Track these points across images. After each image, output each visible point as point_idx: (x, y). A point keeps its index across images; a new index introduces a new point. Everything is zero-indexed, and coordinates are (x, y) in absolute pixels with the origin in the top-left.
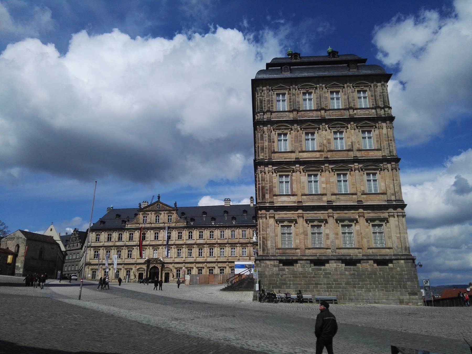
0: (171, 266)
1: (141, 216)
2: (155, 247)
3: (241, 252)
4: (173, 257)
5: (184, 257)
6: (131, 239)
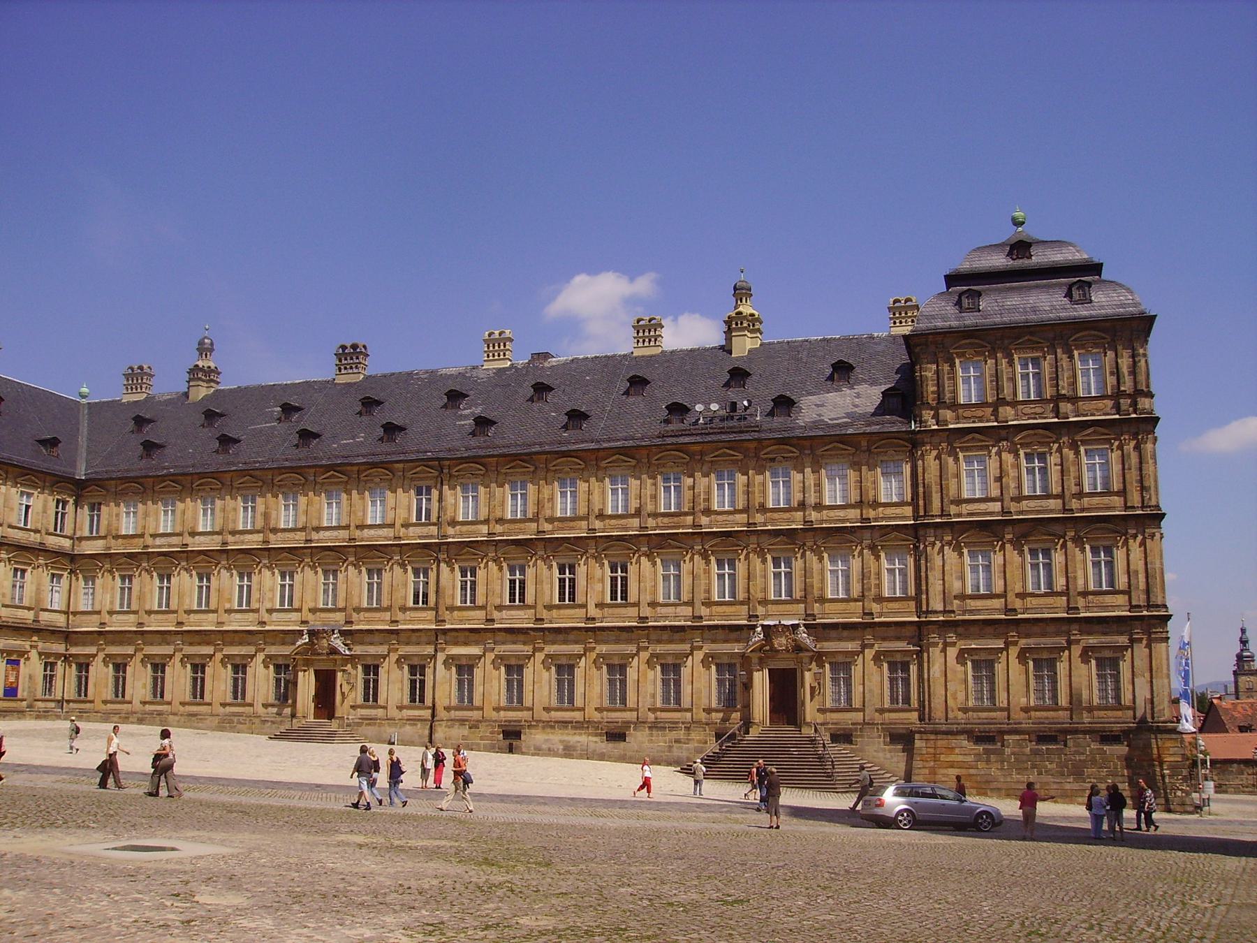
3: (8, 584)
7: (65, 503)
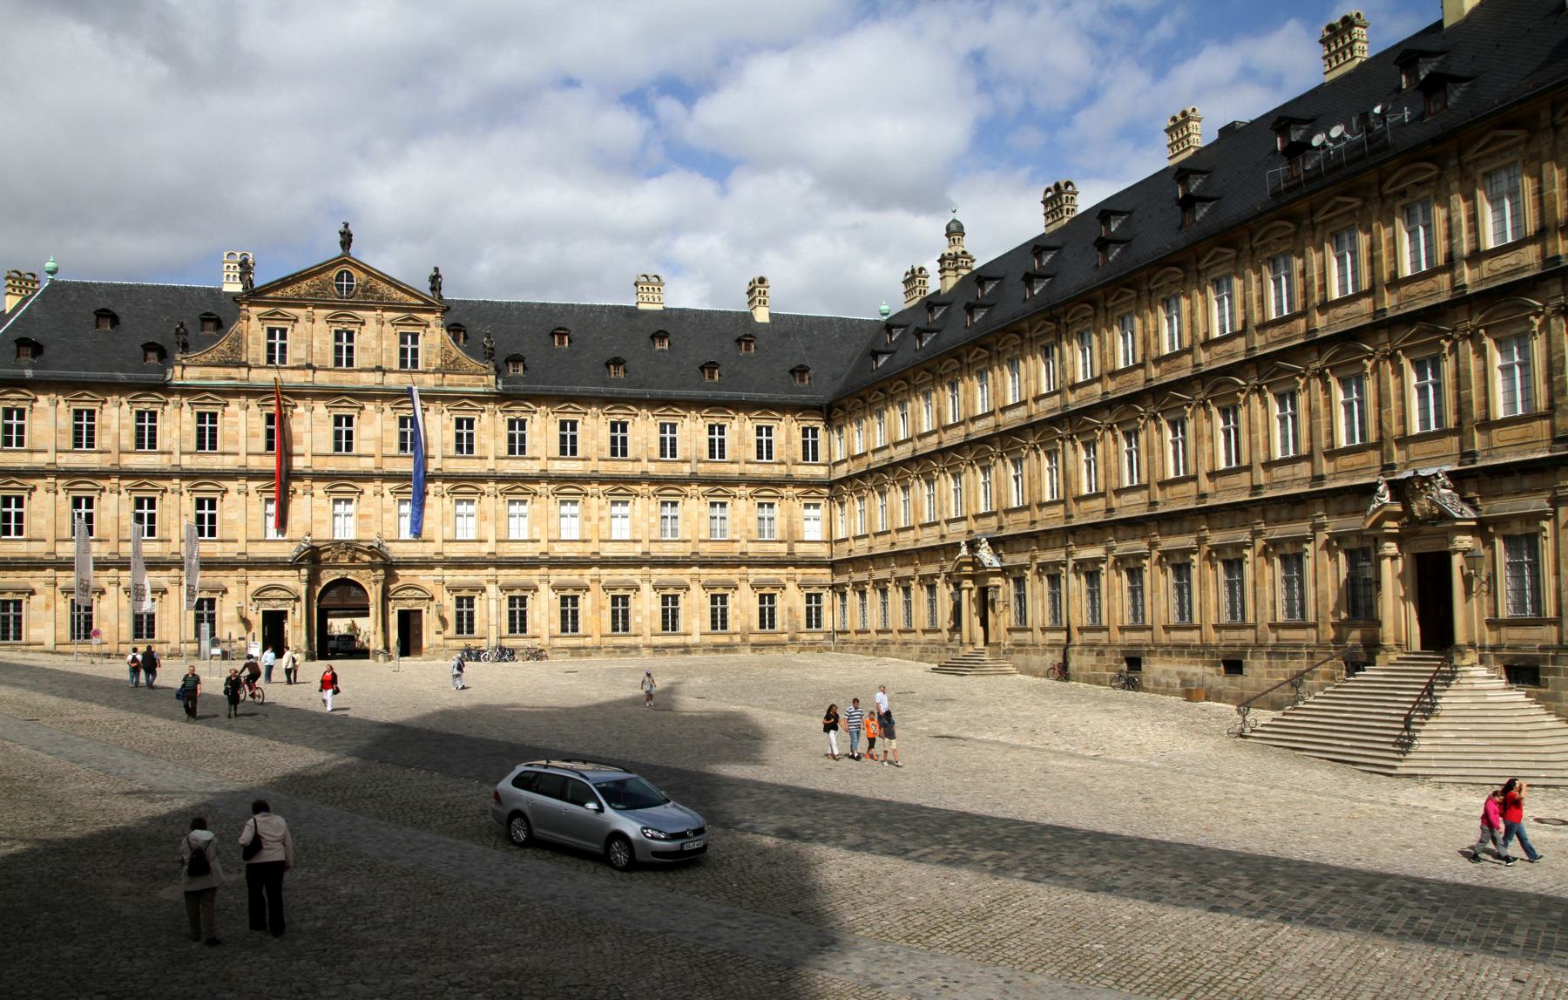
0: (424, 578)
1: (253, 328)
2: (342, 483)
4: (438, 539)
5: (492, 539)
6: (206, 439)
7: (815, 431)
